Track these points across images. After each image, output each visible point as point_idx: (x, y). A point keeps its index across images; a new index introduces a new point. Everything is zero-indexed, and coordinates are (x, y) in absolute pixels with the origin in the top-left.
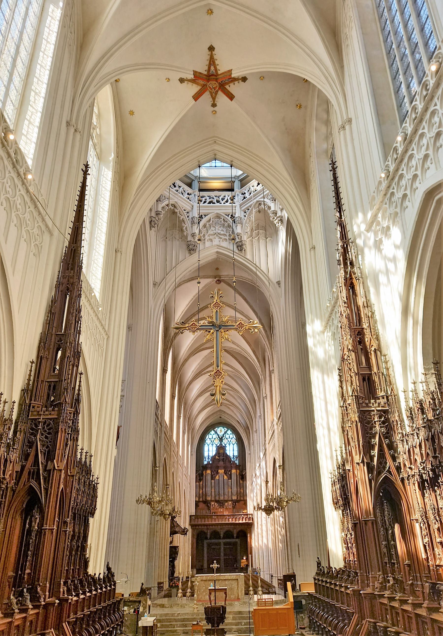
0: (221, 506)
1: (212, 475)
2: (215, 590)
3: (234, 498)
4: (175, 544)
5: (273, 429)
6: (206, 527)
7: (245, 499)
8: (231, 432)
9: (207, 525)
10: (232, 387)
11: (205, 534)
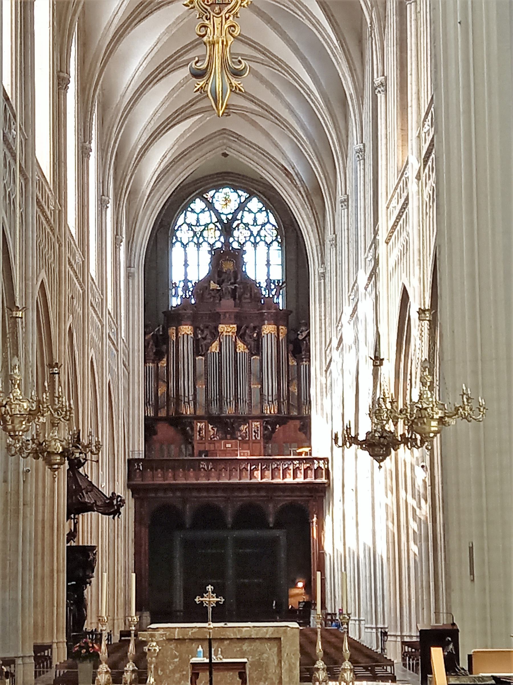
0: (226, 433)
1: (196, 342)
2: (210, 666)
3: (271, 410)
4: (82, 541)
5: (405, 194)
7: (305, 413)
10: (264, 51)
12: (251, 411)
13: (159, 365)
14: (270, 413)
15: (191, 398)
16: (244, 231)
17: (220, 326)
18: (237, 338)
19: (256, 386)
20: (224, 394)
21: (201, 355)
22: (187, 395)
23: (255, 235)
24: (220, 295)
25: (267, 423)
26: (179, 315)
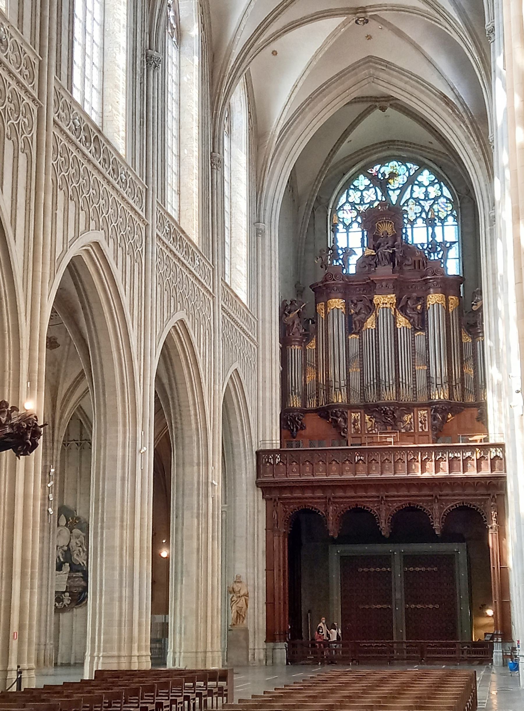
0: (386, 424)
6: (319, 494)
8: (433, 177)
9: (323, 486)
11: (322, 521)
12: (416, 397)
13: (307, 348)
14: (439, 398)
16: (414, 207)
17: (376, 297)
18: (397, 311)
19: (421, 368)
21: (354, 333)
23: (427, 211)
24: (375, 263)
25: (436, 411)
26: (327, 286)
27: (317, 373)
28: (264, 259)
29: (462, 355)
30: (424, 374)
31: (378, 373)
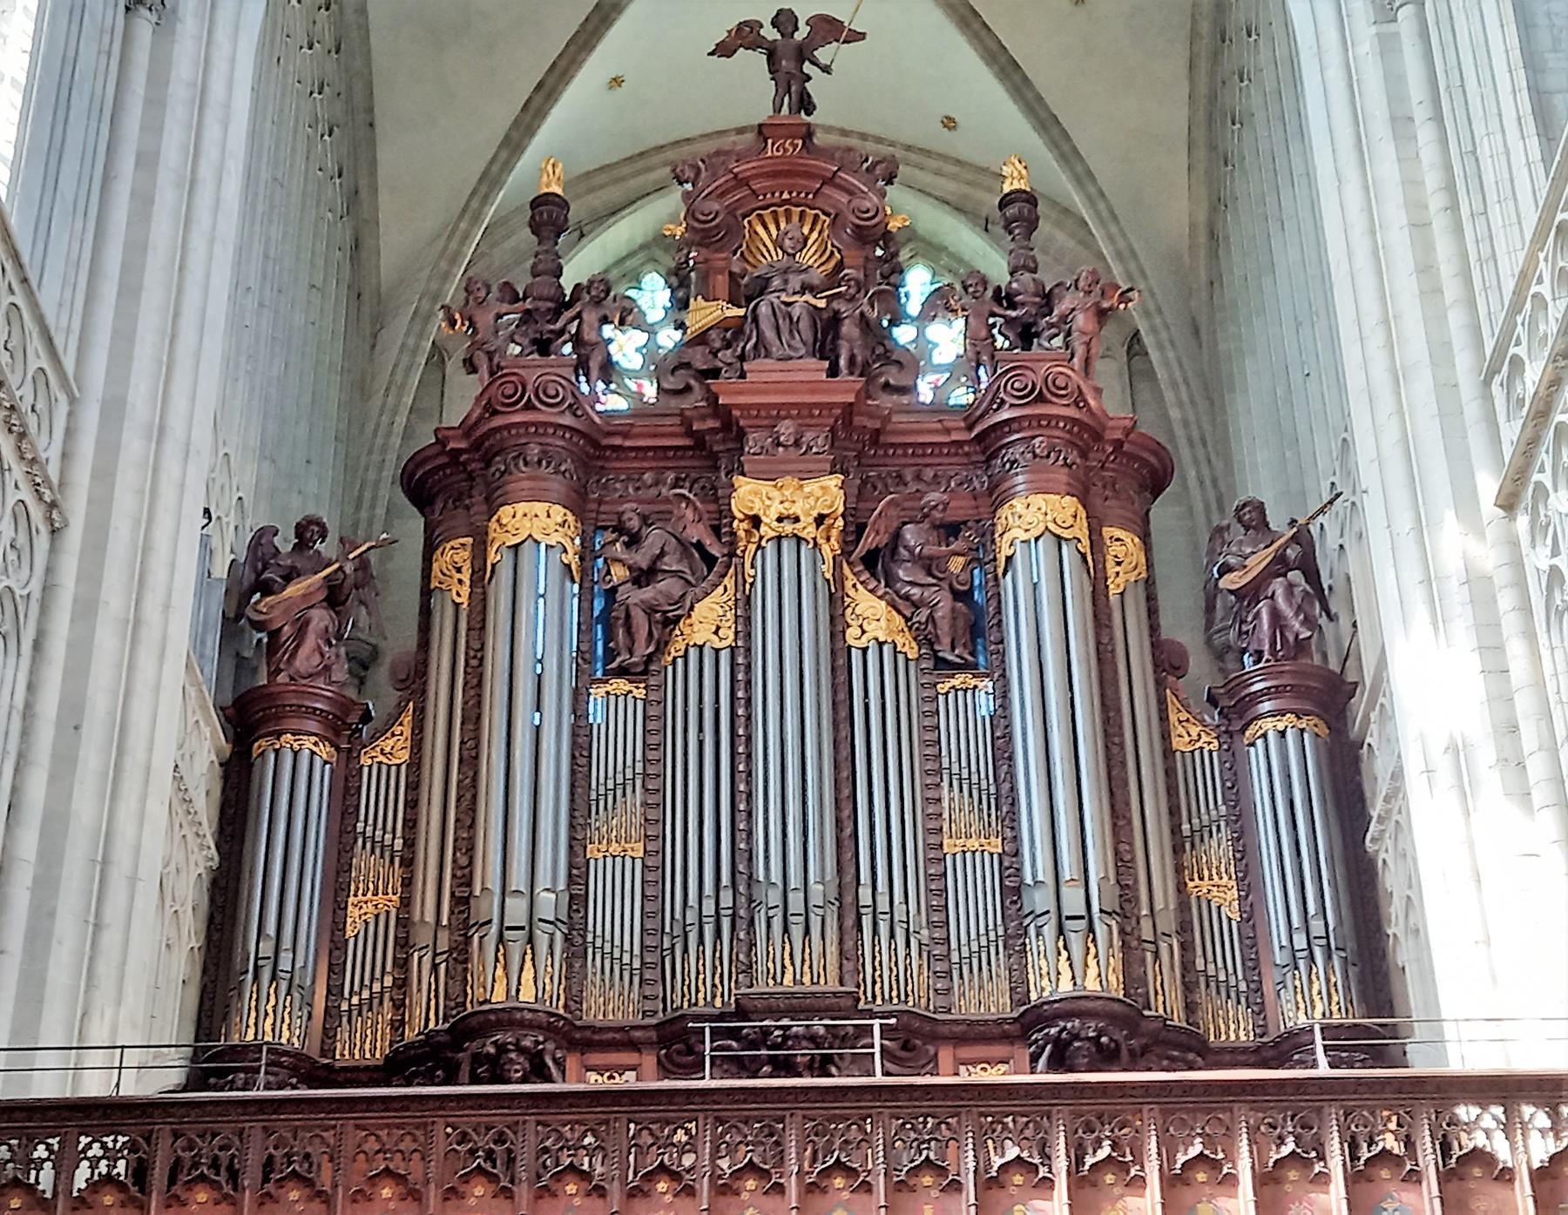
13: (365, 761)
15: (548, 905)
19: (973, 843)
20: (768, 868)
21: (622, 672)
22: (518, 880)
27: (408, 883)
28: (153, 128)
29: (1174, 811)
30: (992, 882)
31: (743, 855)
